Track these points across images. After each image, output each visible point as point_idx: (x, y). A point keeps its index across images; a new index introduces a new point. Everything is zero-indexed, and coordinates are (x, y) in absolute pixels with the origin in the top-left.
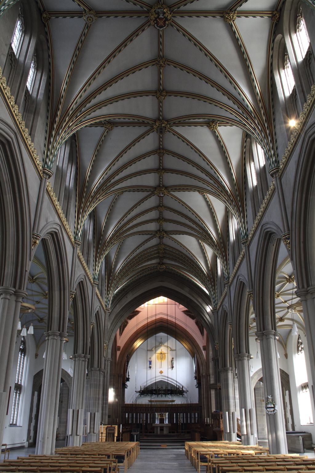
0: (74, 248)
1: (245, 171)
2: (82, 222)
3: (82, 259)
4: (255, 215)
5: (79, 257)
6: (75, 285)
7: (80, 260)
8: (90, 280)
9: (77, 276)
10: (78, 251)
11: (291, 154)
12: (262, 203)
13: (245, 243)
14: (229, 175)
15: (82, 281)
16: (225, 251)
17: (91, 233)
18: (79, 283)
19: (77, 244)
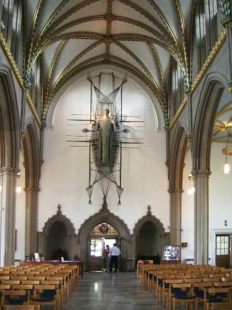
0: (23, 91)
1: (194, 22)
2: (30, 66)
3: (31, 103)
4: (200, 65)
5: (28, 100)
6: (25, 129)
7: (29, 103)
8: (38, 122)
9: (26, 118)
10: (28, 95)
11: (219, 48)
12: (209, 54)
13: (188, 92)
14: (179, 29)
15: (30, 124)
16: (167, 100)
17: (38, 77)
18: (28, 126)
19: (26, 87)
